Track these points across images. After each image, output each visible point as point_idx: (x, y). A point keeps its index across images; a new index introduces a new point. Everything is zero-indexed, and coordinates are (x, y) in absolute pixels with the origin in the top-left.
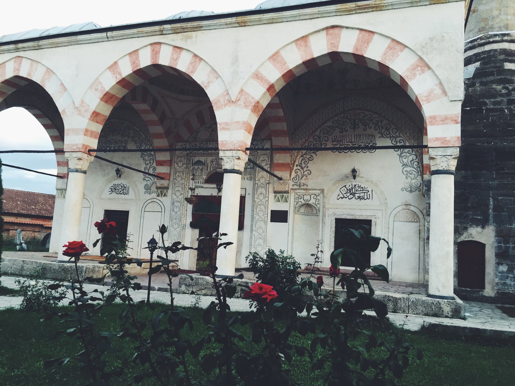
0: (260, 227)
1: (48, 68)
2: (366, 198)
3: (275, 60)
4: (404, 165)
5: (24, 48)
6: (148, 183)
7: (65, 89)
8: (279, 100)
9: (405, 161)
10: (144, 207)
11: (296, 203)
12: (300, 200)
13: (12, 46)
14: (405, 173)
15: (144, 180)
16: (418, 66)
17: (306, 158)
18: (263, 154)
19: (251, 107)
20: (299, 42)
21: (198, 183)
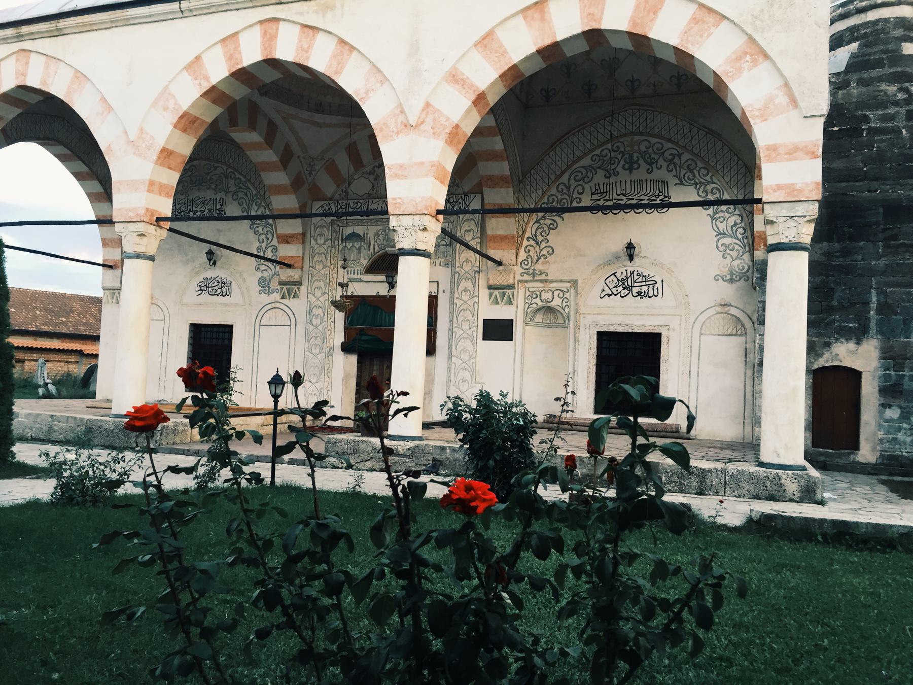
0: (465, 350)
1: (77, 71)
2: (651, 294)
3: (486, 47)
4: (720, 234)
5: (32, 33)
6: (265, 274)
7: (110, 108)
8: (496, 120)
9: (722, 226)
11: (527, 305)
12: (534, 301)
14: (722, 249)
15: (257, 269)
16: (746, 53)
17: (544, 226)
18: (468, 220)
19: (444, 136)
20: (530, 13)
21: (354, 273)
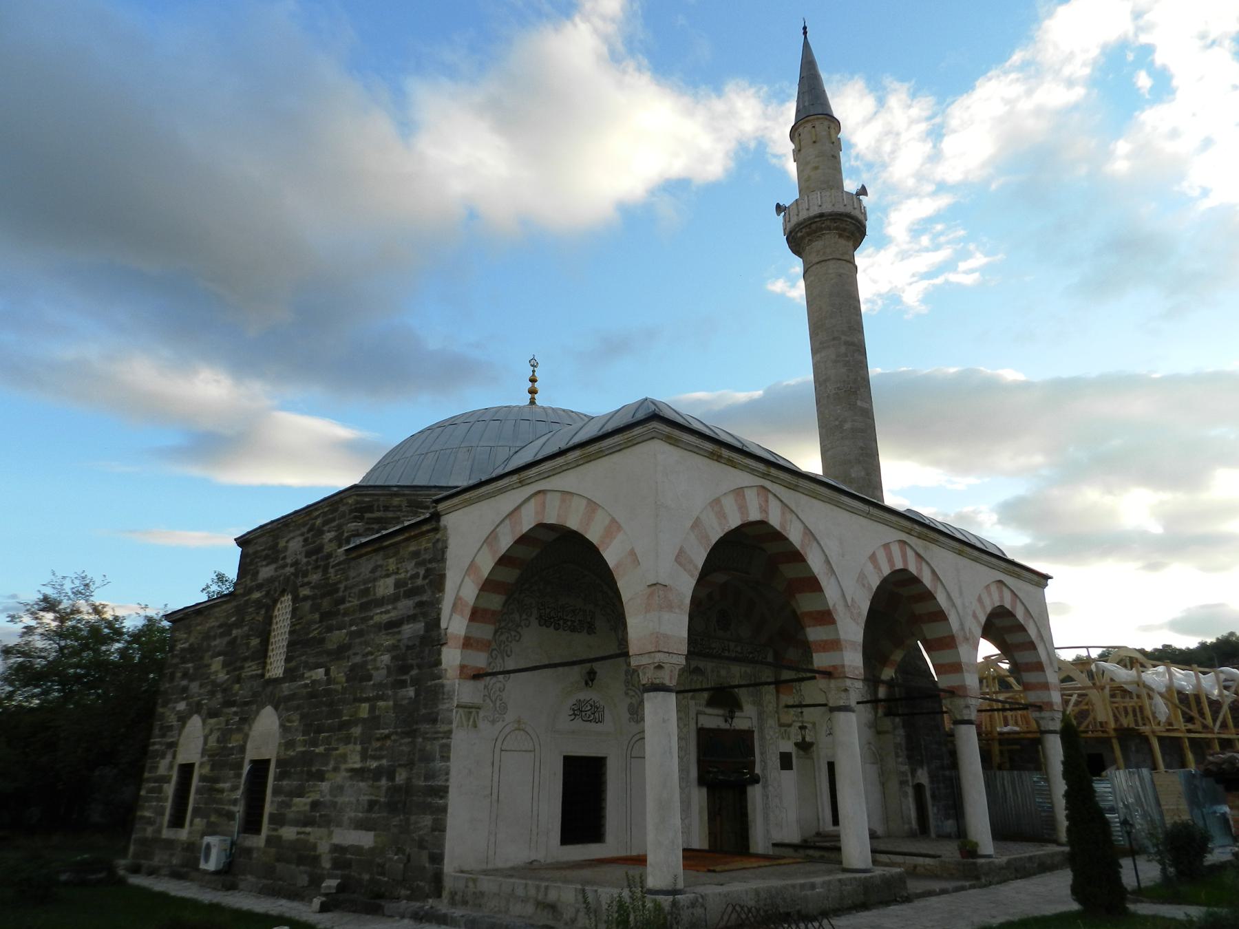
1: (806, 527)
10: (630, 748)
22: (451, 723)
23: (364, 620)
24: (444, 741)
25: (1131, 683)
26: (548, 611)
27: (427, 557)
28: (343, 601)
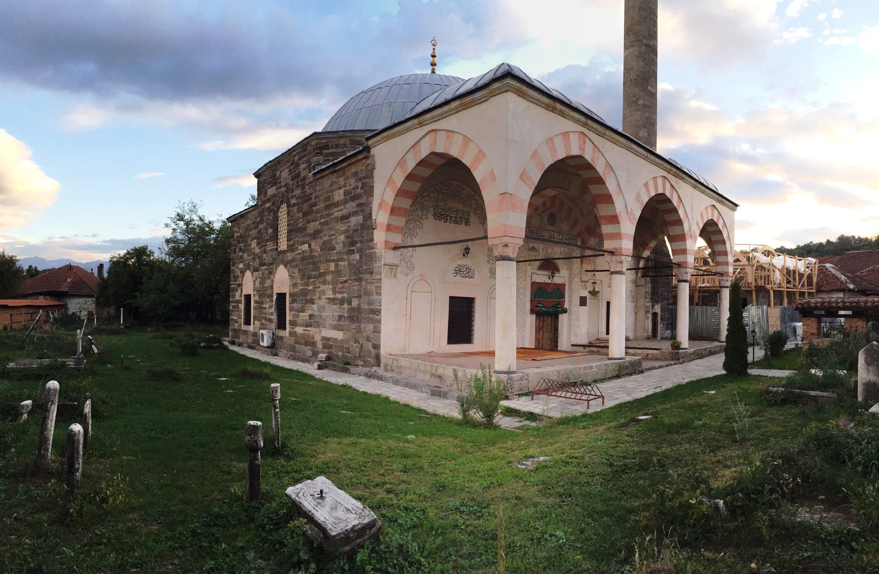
10: (490, 293)
13: (582, 118)
22: (381, 274)
23: (329, 215)
24: (377, 284)
25: (767, 263)
26: (440, 210)
27: (363, 175)
28: (315, 204)
